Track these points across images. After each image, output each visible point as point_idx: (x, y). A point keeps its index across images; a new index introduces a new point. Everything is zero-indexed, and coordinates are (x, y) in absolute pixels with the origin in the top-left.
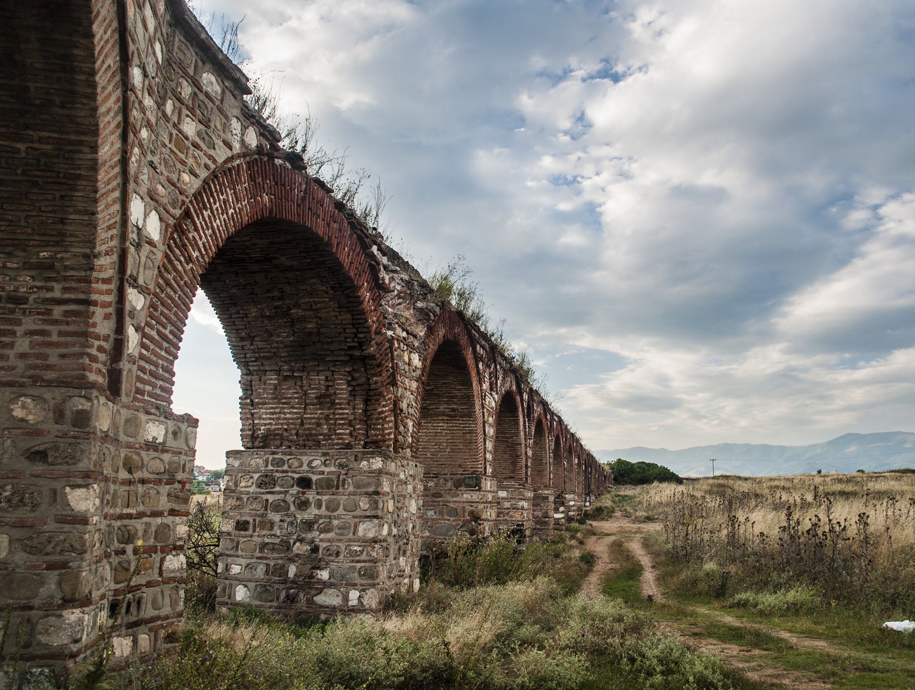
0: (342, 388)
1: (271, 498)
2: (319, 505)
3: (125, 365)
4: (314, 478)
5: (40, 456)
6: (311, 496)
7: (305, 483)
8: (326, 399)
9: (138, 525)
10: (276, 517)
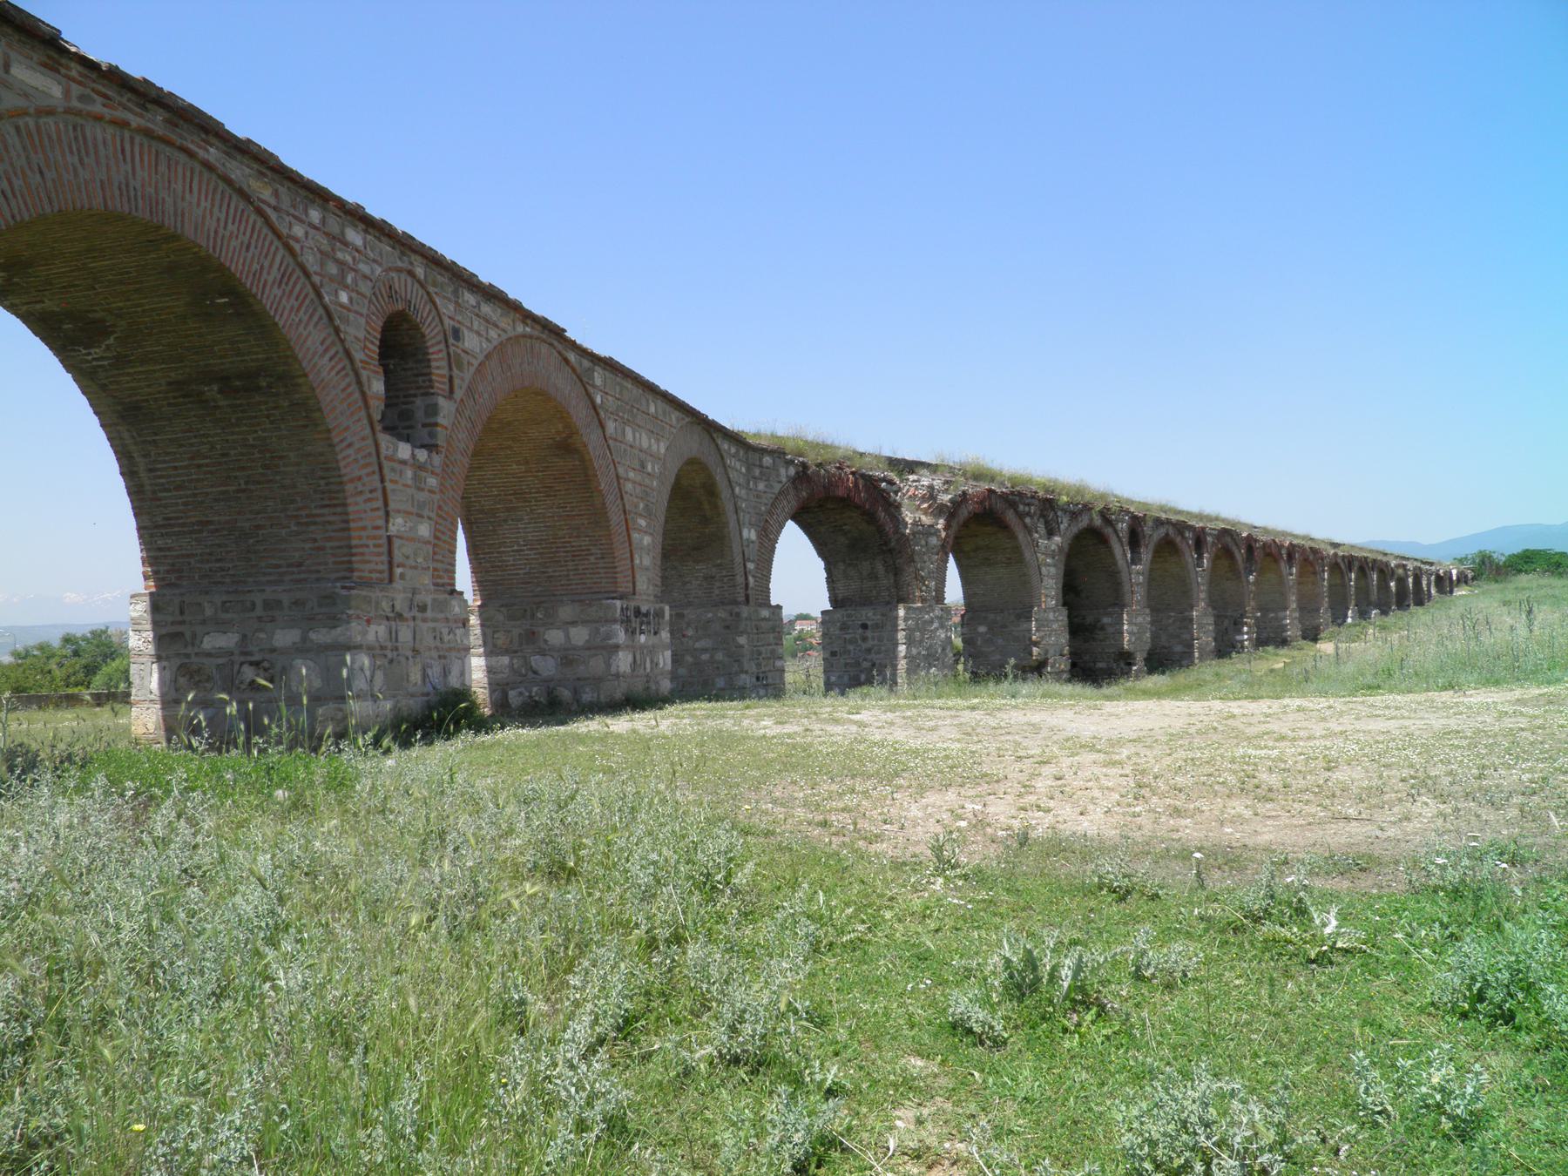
0: (880, 568)
1: (848, 637)
2: (873, 638)
3: (750, 592)
4: (869, 623)
5: (727, 627)
6: (869, 634)
7: (864, 626)
8: (873, 576)
9: (763, 649)
10: (851, 647)
